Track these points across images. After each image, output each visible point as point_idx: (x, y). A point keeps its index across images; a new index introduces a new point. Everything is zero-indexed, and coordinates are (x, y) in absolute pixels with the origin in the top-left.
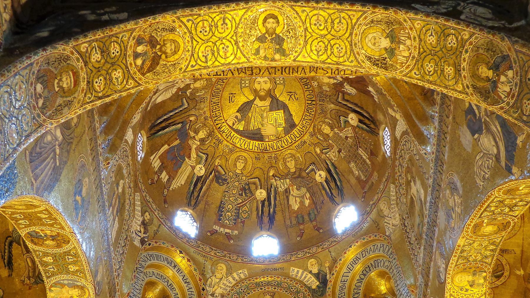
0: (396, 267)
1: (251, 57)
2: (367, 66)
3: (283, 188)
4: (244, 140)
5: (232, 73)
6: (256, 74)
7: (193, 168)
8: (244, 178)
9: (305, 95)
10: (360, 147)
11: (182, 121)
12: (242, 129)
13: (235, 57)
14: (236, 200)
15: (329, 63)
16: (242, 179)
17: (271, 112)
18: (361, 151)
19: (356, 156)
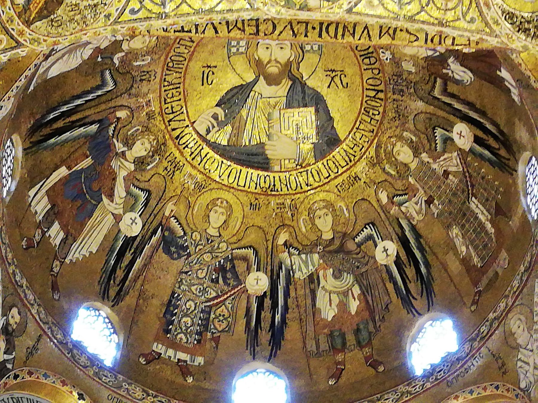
2: (503, 32)
3: (305, 271)
5: (215, 28)
6: (265, 35)
7: (118, 218)
8: (223, 246)
9: (362, 79)
12: (224, 143)
15: (423, 22)
17: (289, 110)
18: (474, 205)
19: (465, 215)
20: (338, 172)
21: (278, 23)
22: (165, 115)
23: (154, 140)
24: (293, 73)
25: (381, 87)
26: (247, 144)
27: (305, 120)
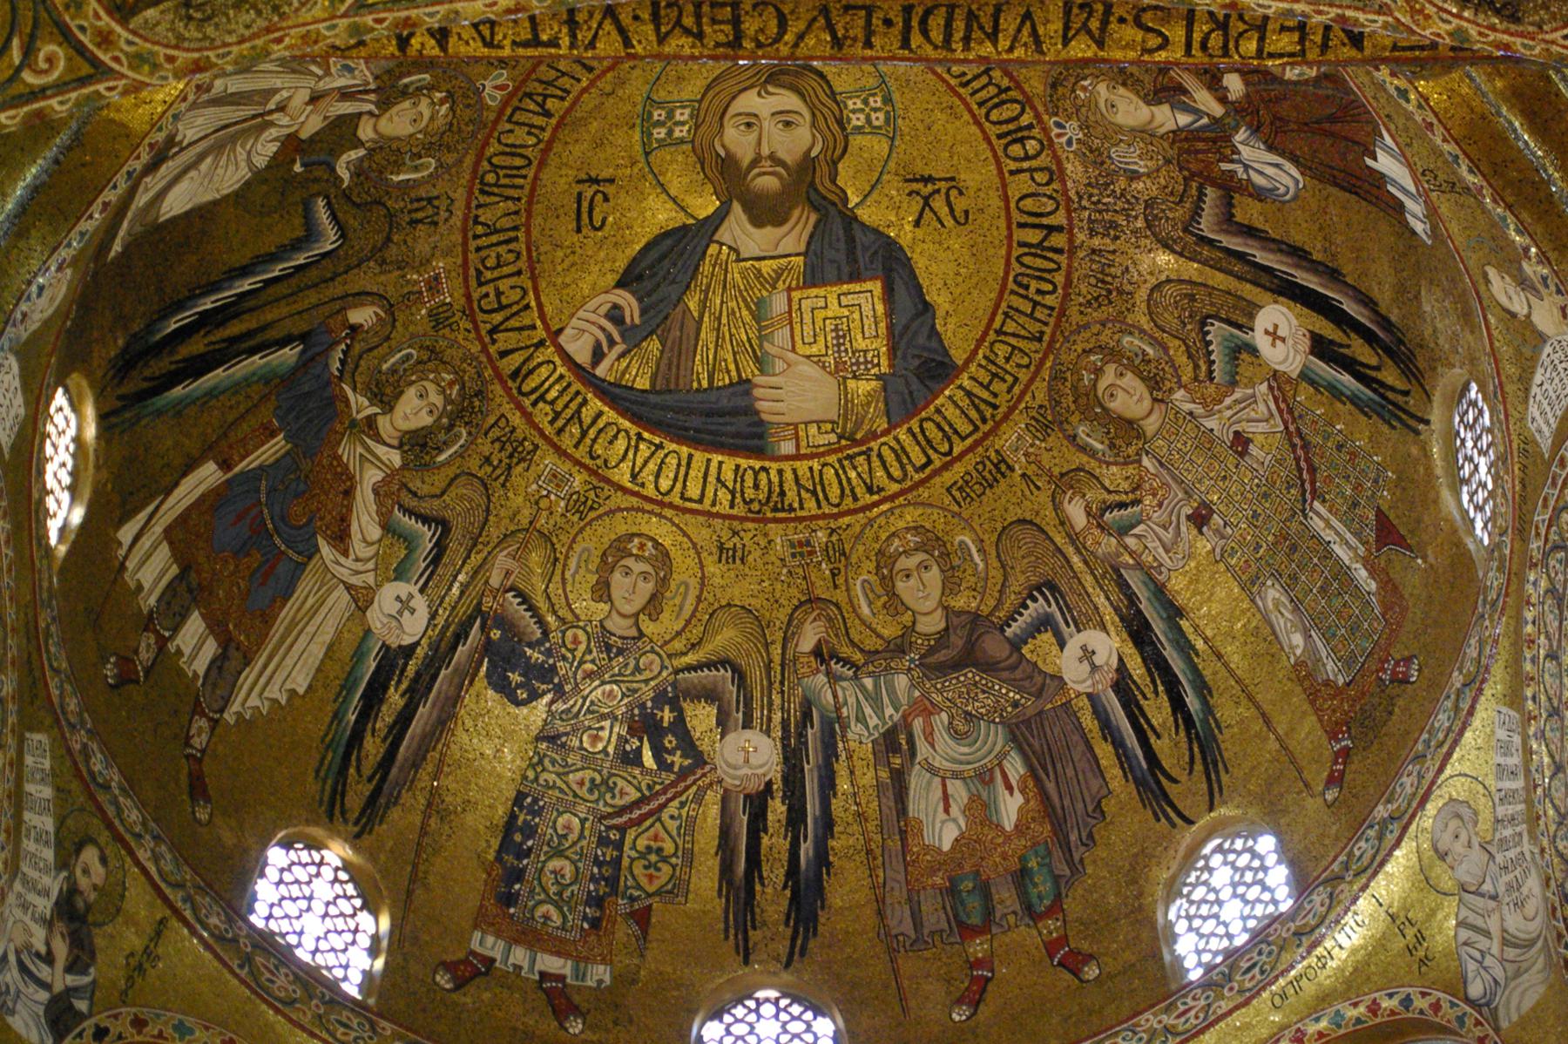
3: (873, 721)
5: (622, 31)
6: (760, 45)
7: (362, 600)
9: (1006, 200)
11: (301, 326)
12: (643, 383)
14: (606, 786)
16: (637, 669)
17: (814, 291)
21: (792, 12)
22: (480, 317)
23: (451, 384)
24: (823, 191)
25: (1060, 219)
26: (705, 384)
27: (856, 316)
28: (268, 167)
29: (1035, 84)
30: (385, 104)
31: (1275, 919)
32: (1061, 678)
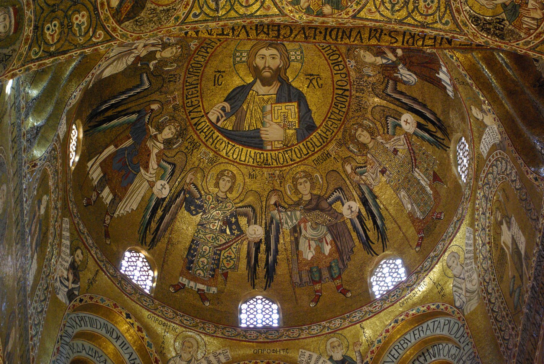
0: (471, 357)
1: (286, 7)
2: (470, 31)
3: (290, 224)
4: (234, 146)
5: (247, 32)
6: (284, 38)
7: (152, 185)
9: (333, 81)
10: (416, 166)
11: (139, 109)
12: (230, 128)
13: (262, 5)
15: (409, 25)
16: (226, 207)
17: (278, 105)
18: (418, 174)
20: (314, 151)
22: (187, 108)
23: (178, 126)
25: (348, 87)
26: (247, 129)
28: (131, 64)
29: (343, 50)
30: (164, 48)
31: (401, 282)
32: (343, 214)
